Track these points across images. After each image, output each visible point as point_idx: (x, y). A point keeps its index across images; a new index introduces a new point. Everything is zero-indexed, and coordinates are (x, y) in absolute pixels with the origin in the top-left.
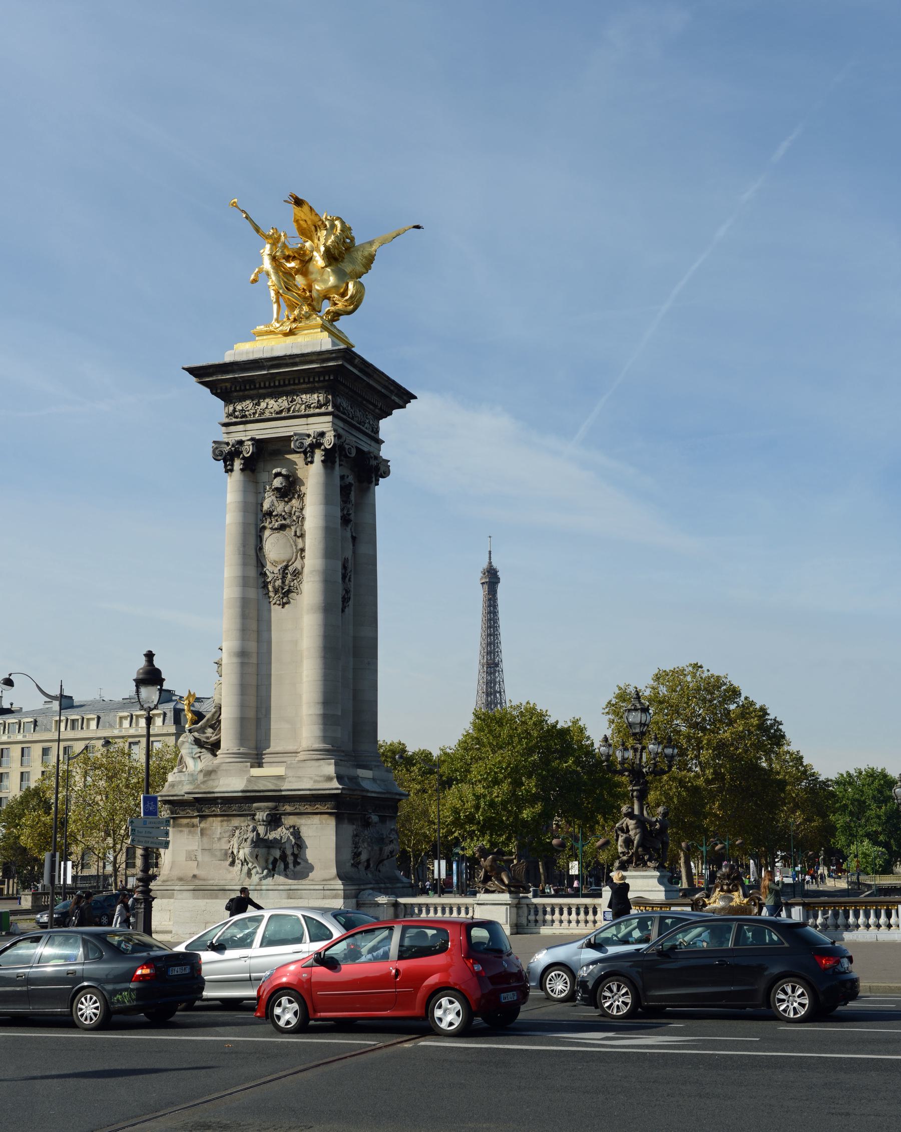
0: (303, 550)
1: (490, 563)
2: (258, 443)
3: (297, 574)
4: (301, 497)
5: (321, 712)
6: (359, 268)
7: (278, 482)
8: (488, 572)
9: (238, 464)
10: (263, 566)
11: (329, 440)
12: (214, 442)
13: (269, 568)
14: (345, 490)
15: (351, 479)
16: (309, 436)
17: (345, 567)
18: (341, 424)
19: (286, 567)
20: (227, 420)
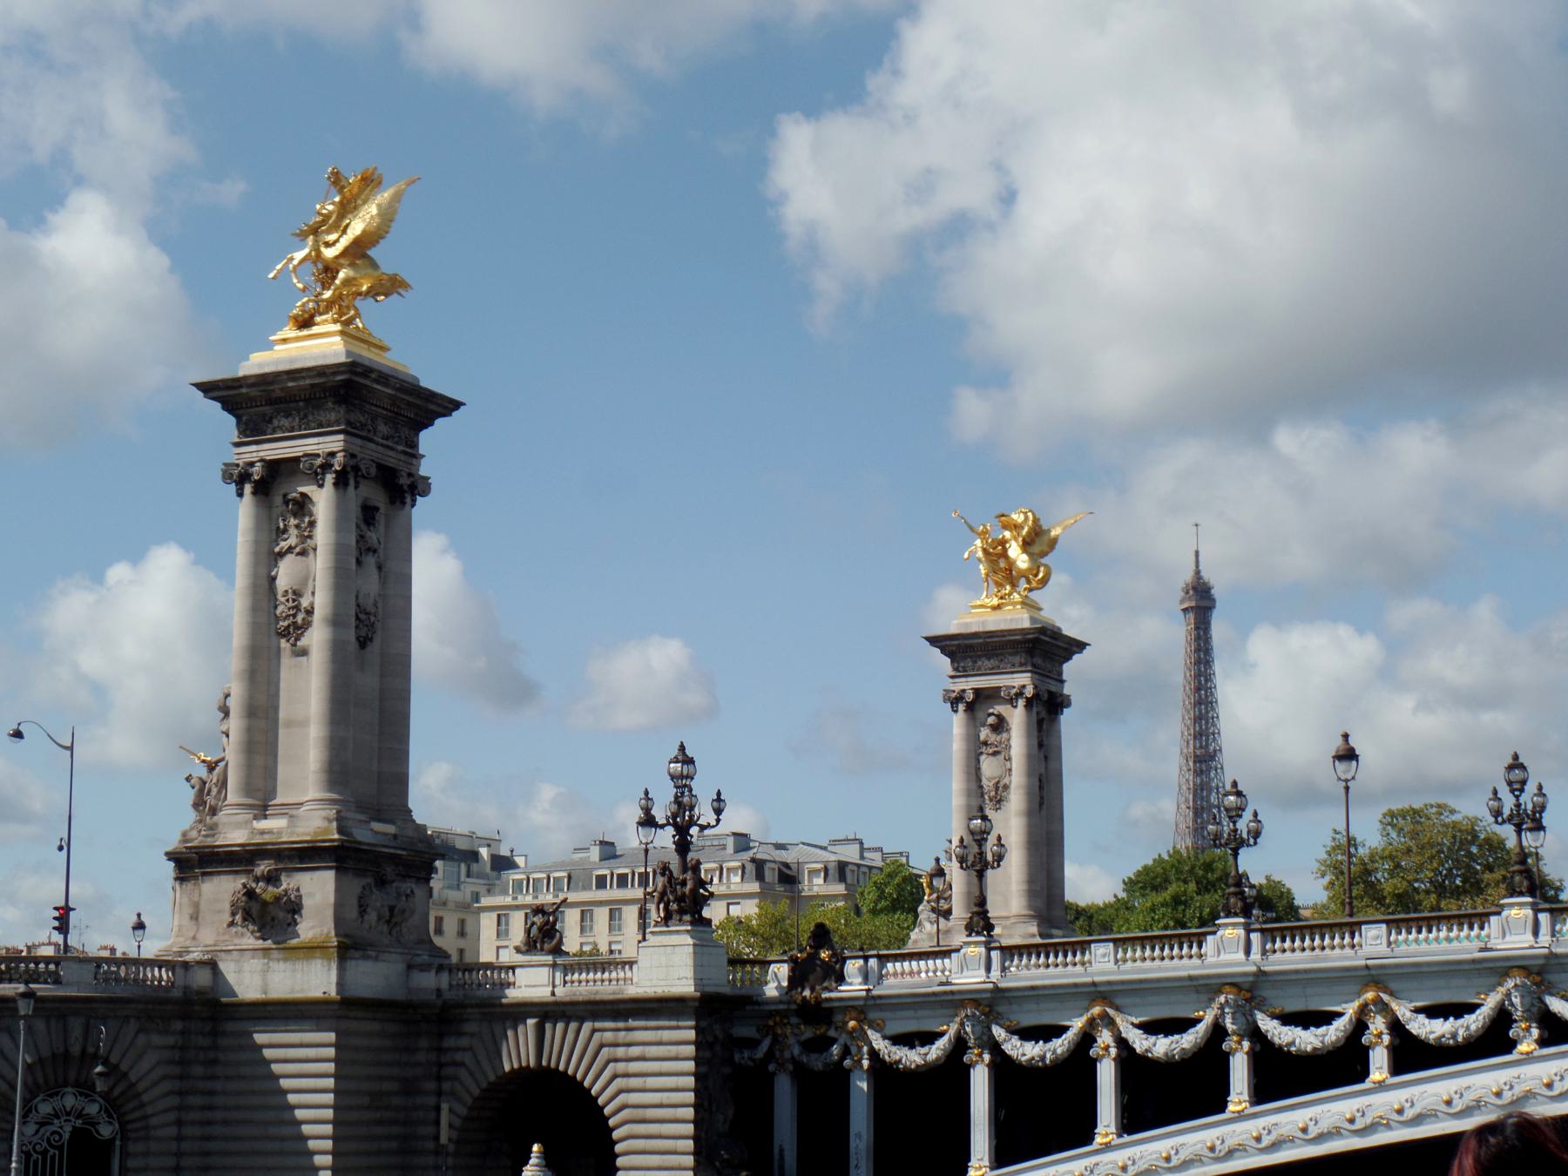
0: (1010, 770)
1: (1198, 572)
2: (977, 692)
3: (1006, 787)
4: (1008, 730)
5: (1027, 888)
6: (1045, 548)
7: (991, 720)
8: (1194, 588)
9: (961, 707)
10: (981, 781)
11: (1029, 691)
12: (944, 690)
13: (985, 782)
14: (1040, 723)
15: (1044, 714)
16: (1014, 687)
17: (1040, 780)
18: (1037, 676)
19: (998, 782)
20: (953, 673)
